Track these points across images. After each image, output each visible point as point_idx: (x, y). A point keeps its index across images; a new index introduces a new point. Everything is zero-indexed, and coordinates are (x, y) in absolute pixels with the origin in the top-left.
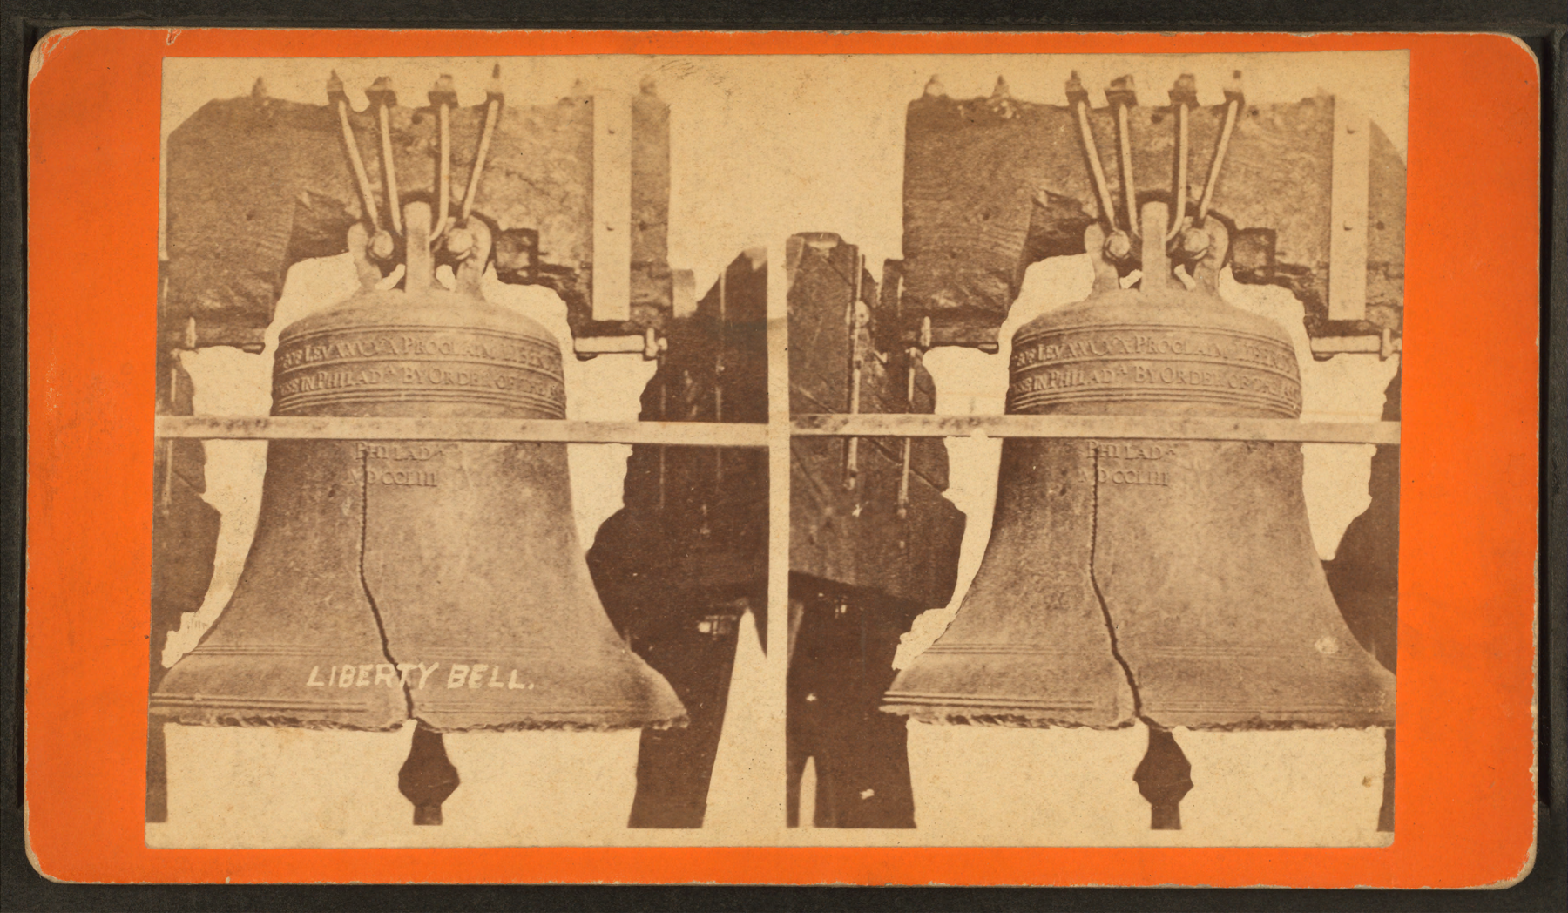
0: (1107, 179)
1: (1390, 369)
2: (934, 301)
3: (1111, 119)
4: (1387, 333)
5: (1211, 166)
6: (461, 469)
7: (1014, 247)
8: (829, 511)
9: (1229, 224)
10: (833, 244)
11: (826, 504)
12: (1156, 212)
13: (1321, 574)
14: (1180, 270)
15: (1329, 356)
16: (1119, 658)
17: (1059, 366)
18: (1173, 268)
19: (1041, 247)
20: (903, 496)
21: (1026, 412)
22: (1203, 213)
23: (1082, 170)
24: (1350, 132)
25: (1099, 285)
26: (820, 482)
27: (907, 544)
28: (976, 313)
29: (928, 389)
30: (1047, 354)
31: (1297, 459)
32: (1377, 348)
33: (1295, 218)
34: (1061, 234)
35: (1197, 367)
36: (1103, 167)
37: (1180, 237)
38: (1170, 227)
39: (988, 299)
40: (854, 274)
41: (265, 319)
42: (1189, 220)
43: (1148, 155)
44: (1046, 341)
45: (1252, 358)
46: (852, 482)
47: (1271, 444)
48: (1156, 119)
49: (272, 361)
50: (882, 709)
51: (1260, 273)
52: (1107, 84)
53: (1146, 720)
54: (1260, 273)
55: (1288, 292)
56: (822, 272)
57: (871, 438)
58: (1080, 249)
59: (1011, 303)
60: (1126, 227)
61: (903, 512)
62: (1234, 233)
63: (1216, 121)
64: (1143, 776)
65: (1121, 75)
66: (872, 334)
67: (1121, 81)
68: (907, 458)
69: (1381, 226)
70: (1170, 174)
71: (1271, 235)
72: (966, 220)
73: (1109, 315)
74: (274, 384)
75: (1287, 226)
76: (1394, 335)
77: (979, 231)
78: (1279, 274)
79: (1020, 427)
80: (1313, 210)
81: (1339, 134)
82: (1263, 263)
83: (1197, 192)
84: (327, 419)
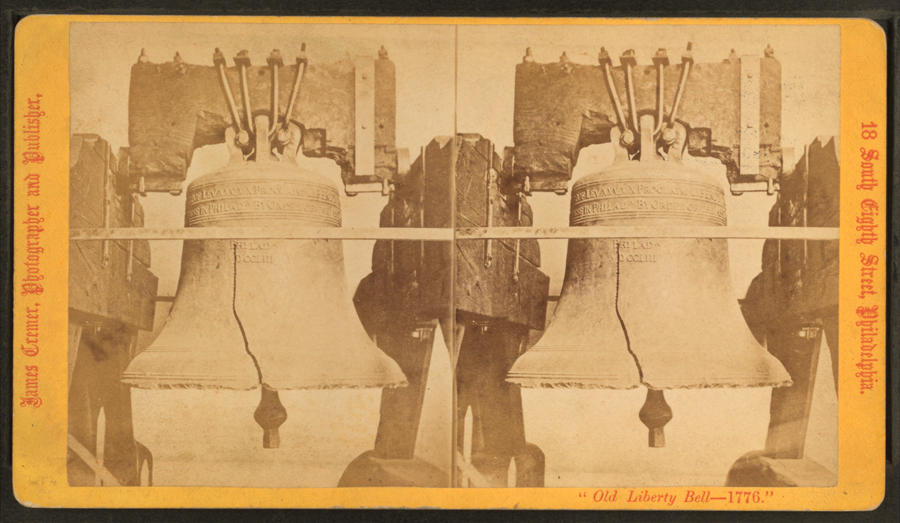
0: (622, 103)
1: (773, 200)
2: (531, 168)
3: (623, 72)
4: (771, 181)
5: (676, 96)
8: (478, 278)
9: (687, 126)
10: (478, 140)
11: (476, 274)
12: (648, 120)
13: (737, 307)
14: (661, 150)
15: (740, 193)
16: (631, 352)
18: (657, 148)
21: (580, 225)
22: (672, 120)
23: (609, 100)
24: (749, 77)
25: (618, 157)
26: (473, 264)
27: (519, 295)
28: (554, 174)
29: (528, 213)
30: (590, 194)
32: (766, 189)
33: (722, 122)
37: (661, 133)
38: (655, 127)
39: (559, 166)
40: (489, 153)
41: (181, 177)
42: (665, 124)
43: (643, 91)
44: (591, 187)
46: (490, 262)
47: (711, 239)
48: (647, 72)
49: (185, 199)
50: (507, 380)
53: (647, 384)
54: (704, 151)
56: (472, 153)
57: (499, 240)
59: (572, 168)
60: (631, 127)
61: (516, 278)
63: (679, 73)
64: (644, 416)
66: (498, 185)
67: (628, 52)
69: (767, 125)
70: (655, 101)
72: (548, 126)
75: (717, 127)
76: (775, 182)
77: (555, 131)
78: (713, 151)
79: (578, 233)
80: (731, 118)
81: (744, 79)
82: (705, 145)
83: (669, 110)
84: (215, 228)
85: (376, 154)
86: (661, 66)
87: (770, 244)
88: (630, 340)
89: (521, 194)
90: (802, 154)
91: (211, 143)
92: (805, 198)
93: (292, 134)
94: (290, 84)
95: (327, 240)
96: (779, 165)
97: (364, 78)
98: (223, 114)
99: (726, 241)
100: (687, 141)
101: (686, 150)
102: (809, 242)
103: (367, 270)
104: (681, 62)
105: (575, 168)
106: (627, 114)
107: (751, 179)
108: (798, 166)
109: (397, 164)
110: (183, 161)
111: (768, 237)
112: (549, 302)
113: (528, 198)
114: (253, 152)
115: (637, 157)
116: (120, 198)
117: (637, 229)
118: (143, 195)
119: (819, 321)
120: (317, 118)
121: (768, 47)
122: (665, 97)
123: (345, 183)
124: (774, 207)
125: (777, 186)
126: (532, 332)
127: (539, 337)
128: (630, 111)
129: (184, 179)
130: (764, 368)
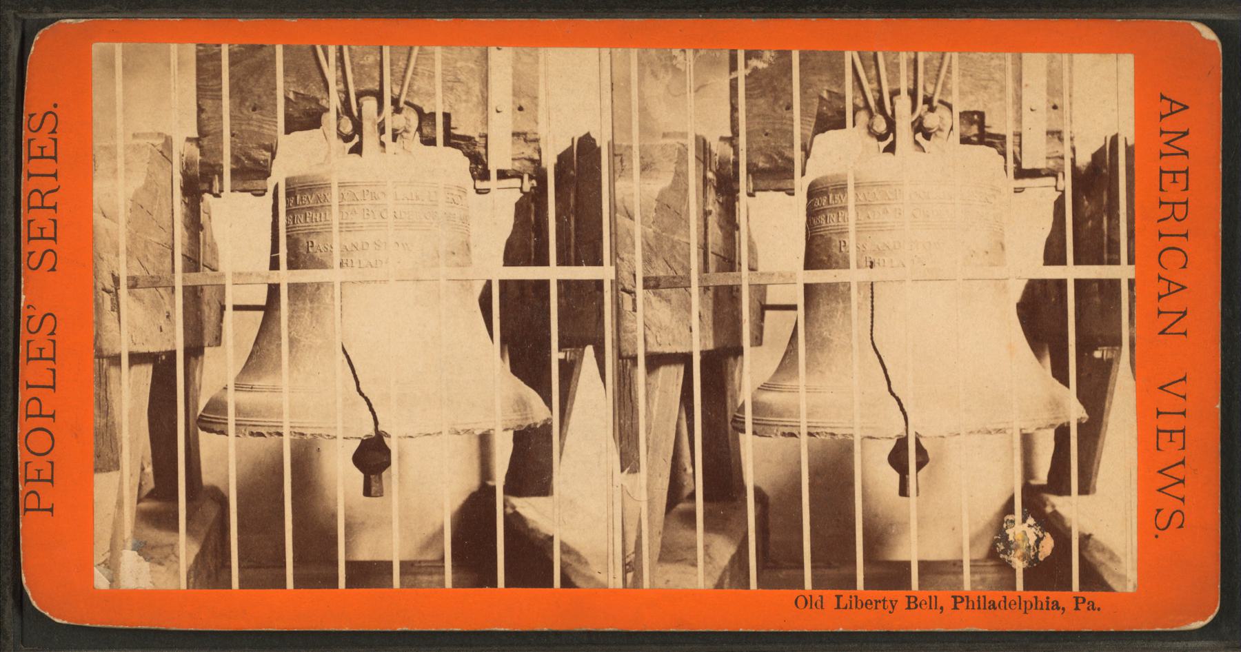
14: (919, 136)
22: (935, 103)
36: (866, 72)
37: (921, 118)
38: (914, 109)
42: (926, 107)
51: (975, 139)
54: (975, 139)
71: (982, 115)
78: (987, 140)
83: (930, 89)
90: (1102, 144)
94: (403, 57)
98: (319, 96)
106: (877, 95)
107: (1035, 173)
108: (1094, 156)
110: (268, 154)
122: (926, 72)
128: (880, 91)
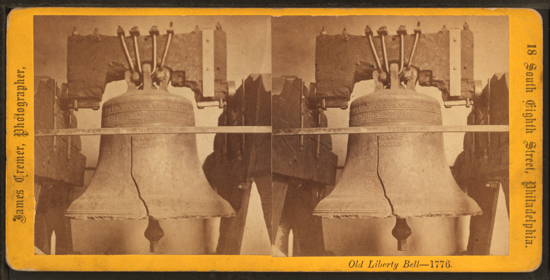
0: (379, 57)
1: (470, 110)
4: (468, 99)
5: (411, 52)
6: (162, 142)
7: (350, 78)
12: (395, 66)
13: (449, 171)
14: (403, 83)
15: (450, 107)
17: (365, 112)
18: (401, 81)
19: (359, 77)
20: (318, 151)
21: (356, 126)
22: (409, 66)
25: (377, 88)
28: (340, 98)
31: (441, 139)
33: (438, 67)
34: (366, 74)
35: (409, 111)
36: (377, 53)
39: (342, 93)
44: (362, 105)
45: (426, 108)
47: (433, 133)
48: (394, 39)
50: (313, 214)
51: (428, 83)
52: (378, 29)
54: (428, 83)
55: (437, 88)
58: (370, 77)
59: (350, 95)
61: (318, 156)
62: (419, 71)
63: (413, 39)
65: (383, 26)
66: (307, 105)
67: (382, 28)
68: (319, 141)
69: (465, 68)
71: (431, 72)
73: (381, 97)
74: (102, 119)
76: (470, 100)
83: (407, 60)
85: (215, 84)
86: (402, 36)
87: (468, 136)
88: (386, 190)
89: (320, 109)
90: (486, 83)
91: (116, 80)
92: (489, 108)
93: (165, 74)
95: (186, 134)
96: (473, 90)
97: (207, 41)
98: (123, 63)
99: (442, 134)
100: (418, 78)
101: (418, 83)
102: (492, 133)
103: (210, 150)
104: (413, 33)
105: (352, 94)
107: (456, 98)
108: (484, 90)
109: (228, 89)
110: (100, 90)
111: (468, 130)
112: (338, 170)
113: (325, 112)
114: (142, 84)
115: (389, 87)
116: (62, 112)
117: (388, 128)
118: (76, 110)
119: (498, 178)
120: (179, 65)
121: (466, 23)
122: (405, 53)
123: (197, 101)
124: (470, 114)
125: (472, 102)
126: (327, 186)
127: (331, 190)
129: (101, 101)
130: (465, 205)
